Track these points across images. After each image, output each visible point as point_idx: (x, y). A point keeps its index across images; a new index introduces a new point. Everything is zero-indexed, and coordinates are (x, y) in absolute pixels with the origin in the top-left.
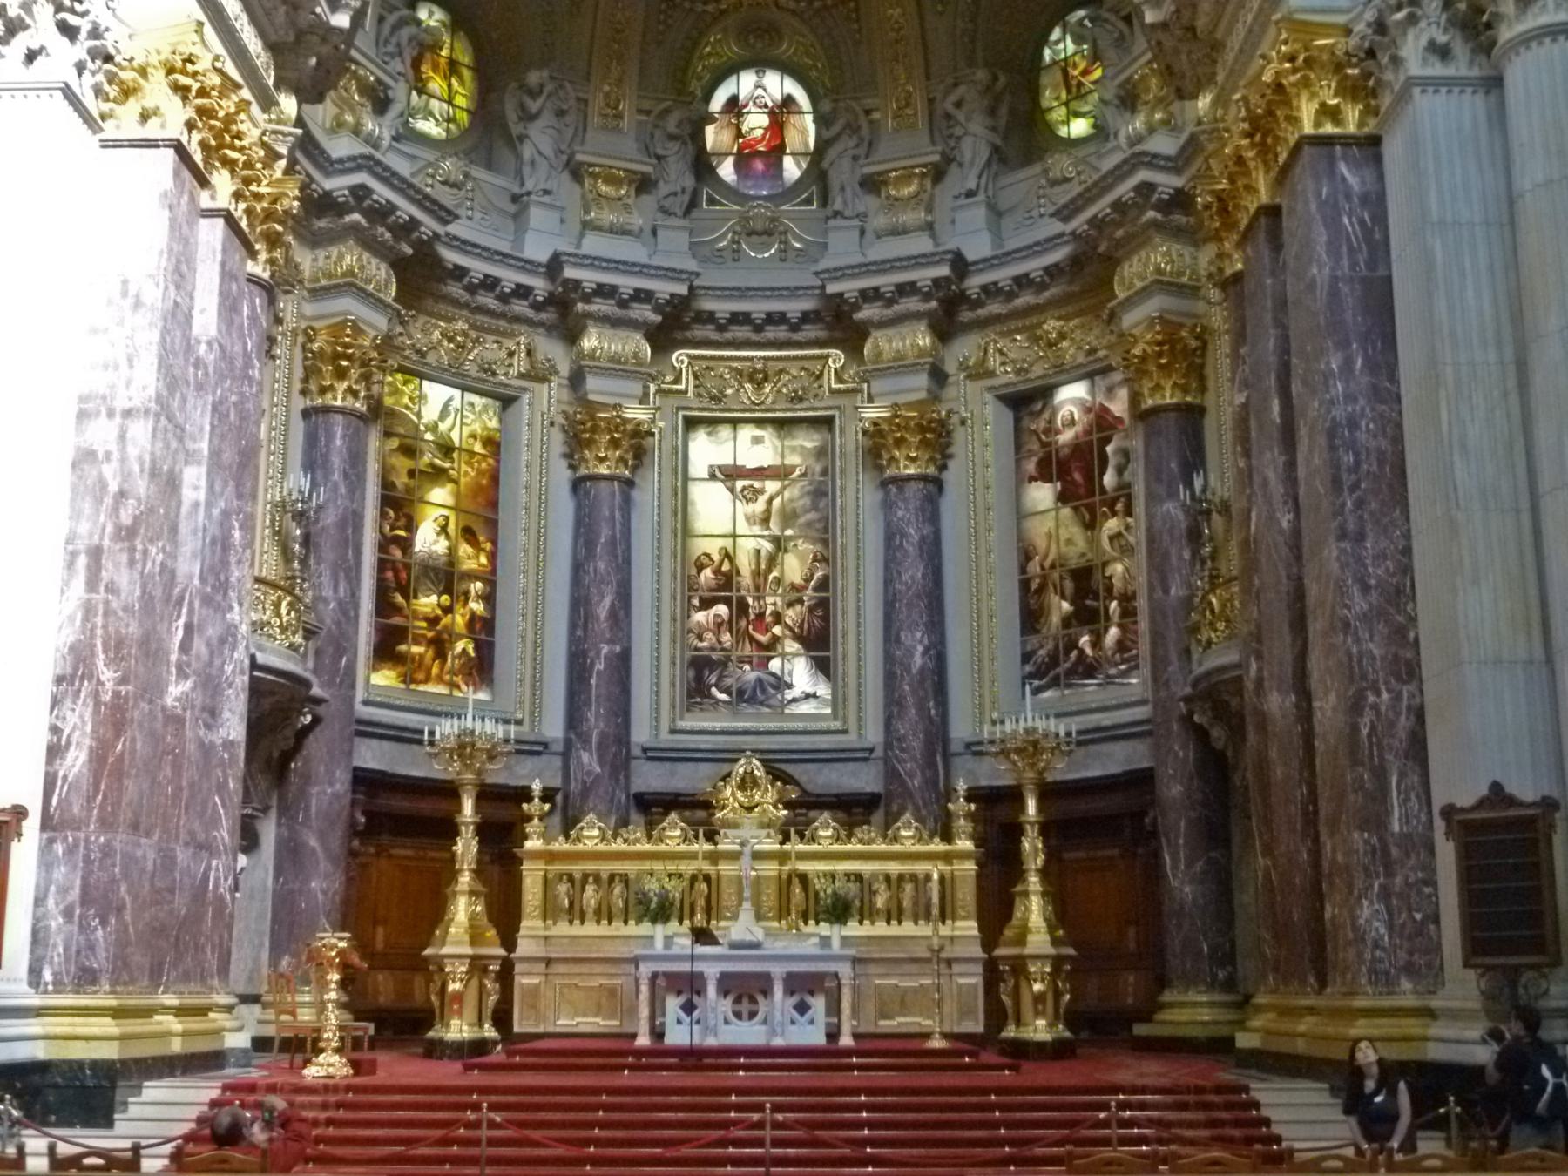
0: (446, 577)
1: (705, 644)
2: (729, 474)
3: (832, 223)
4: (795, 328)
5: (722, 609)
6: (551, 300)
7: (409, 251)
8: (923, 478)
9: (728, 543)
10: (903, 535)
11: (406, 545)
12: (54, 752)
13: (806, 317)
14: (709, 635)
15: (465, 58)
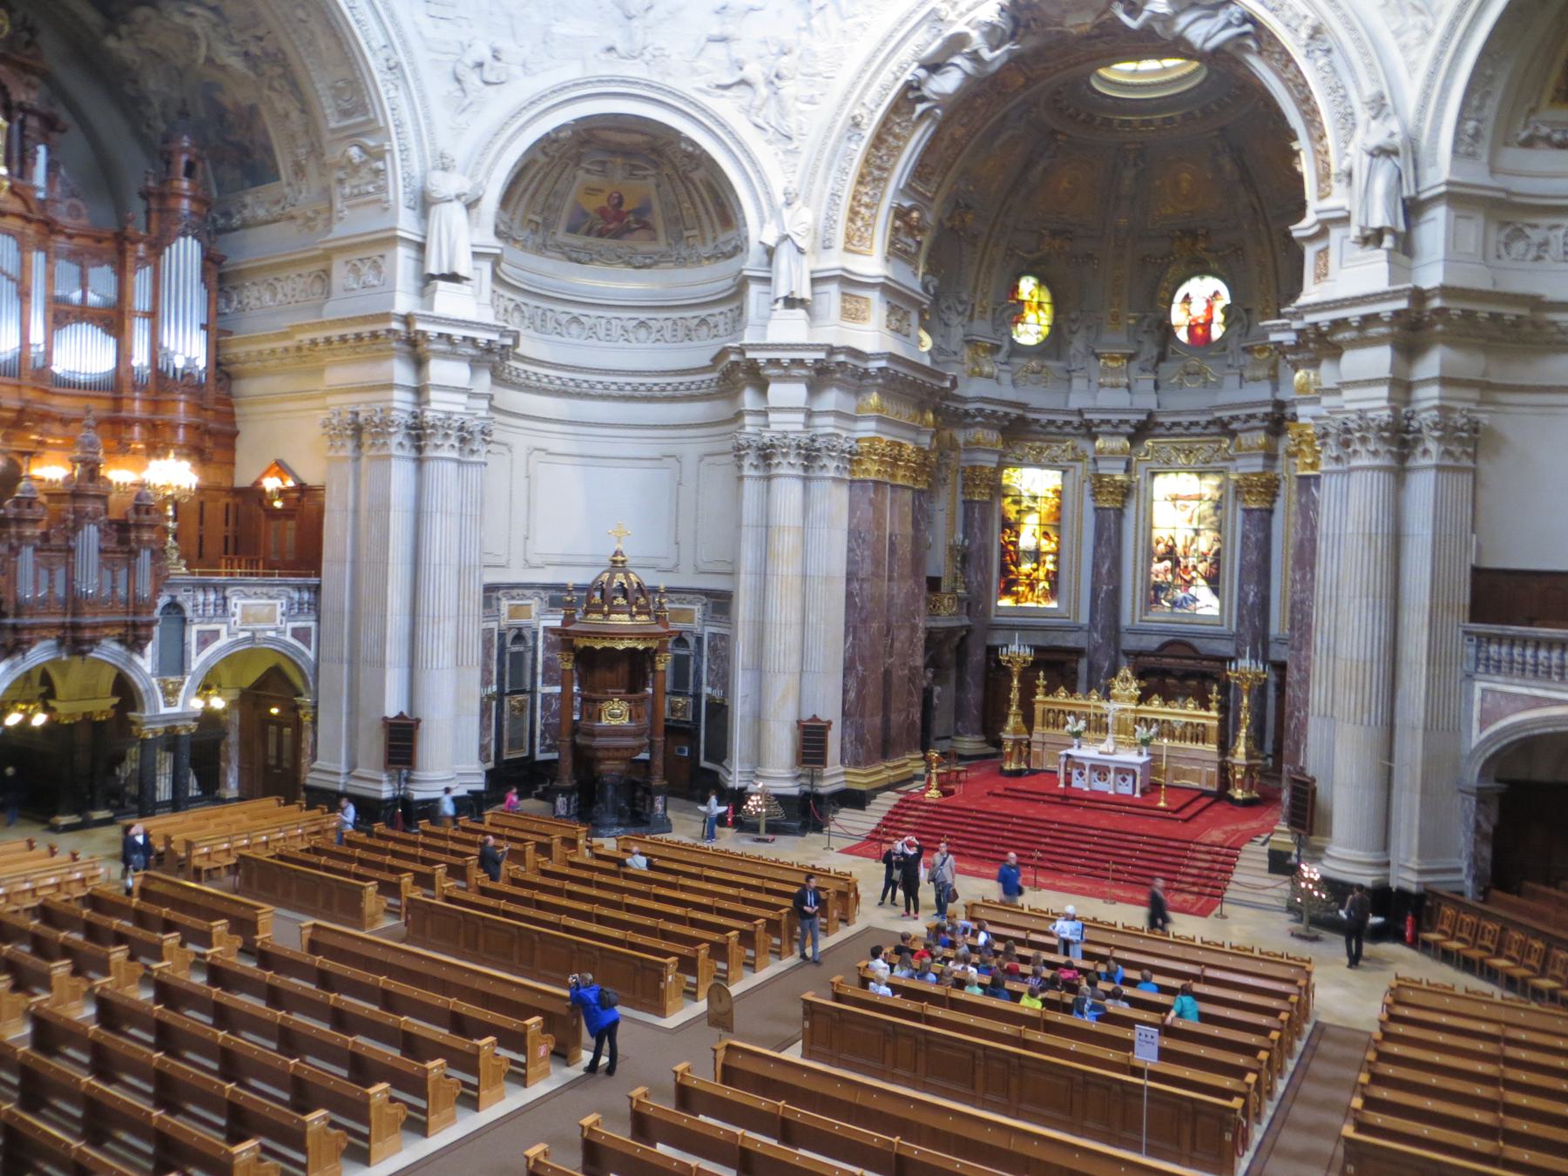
0: (1036, 556)
1: (1159, 580)
2: (1175, 499)
3: (1228, 371)
4: (1205, 427)
5: (1168, 564)
6: (1081, 425)
7: (1006, 423)
8: (1260, 510)
9: (1172, 533)
10: (1248, 538)
11: (1015, 544)
12: (845, 692)
13: (1209, 423)
14: (1161, 575)
15: (1045, 297)
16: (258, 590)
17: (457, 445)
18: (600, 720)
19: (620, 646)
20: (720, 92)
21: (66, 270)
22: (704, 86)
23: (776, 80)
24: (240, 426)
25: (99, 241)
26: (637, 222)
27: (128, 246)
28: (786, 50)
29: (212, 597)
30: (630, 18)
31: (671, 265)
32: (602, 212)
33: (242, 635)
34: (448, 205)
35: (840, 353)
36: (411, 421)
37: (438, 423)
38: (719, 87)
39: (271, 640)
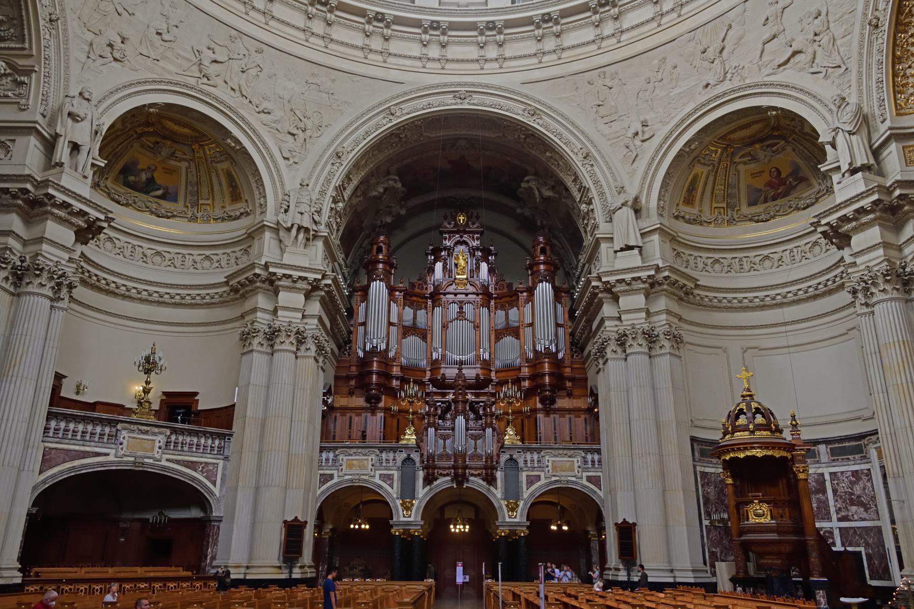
16: (561, 452)
17: (644, 343)
18: (748, 519)
19: (742, 456)
20: (782, 68)
21: (501, 313)
22: (771, 71)
23: (817, 38)
24: (588, 375)
25: (511, 297)
26: (795, 180)
27: (520, 294)
28: (815, 16)
29: (535, 456)
30: (713, 62)
31: (826, 196)
32: (770, 184)
33: (554, 479)
34: (619, 211)
35: (895, 188)
36: (617, 337)
37: (627, 332)
38: (779, 66)
39: (573, 482)
